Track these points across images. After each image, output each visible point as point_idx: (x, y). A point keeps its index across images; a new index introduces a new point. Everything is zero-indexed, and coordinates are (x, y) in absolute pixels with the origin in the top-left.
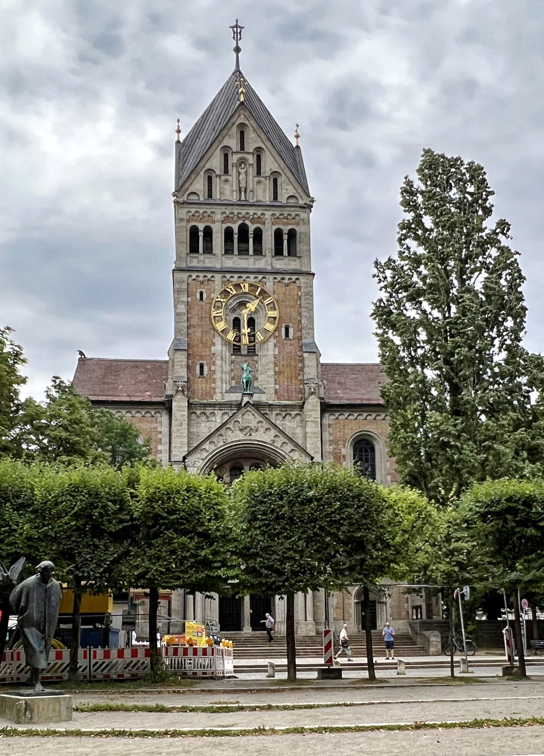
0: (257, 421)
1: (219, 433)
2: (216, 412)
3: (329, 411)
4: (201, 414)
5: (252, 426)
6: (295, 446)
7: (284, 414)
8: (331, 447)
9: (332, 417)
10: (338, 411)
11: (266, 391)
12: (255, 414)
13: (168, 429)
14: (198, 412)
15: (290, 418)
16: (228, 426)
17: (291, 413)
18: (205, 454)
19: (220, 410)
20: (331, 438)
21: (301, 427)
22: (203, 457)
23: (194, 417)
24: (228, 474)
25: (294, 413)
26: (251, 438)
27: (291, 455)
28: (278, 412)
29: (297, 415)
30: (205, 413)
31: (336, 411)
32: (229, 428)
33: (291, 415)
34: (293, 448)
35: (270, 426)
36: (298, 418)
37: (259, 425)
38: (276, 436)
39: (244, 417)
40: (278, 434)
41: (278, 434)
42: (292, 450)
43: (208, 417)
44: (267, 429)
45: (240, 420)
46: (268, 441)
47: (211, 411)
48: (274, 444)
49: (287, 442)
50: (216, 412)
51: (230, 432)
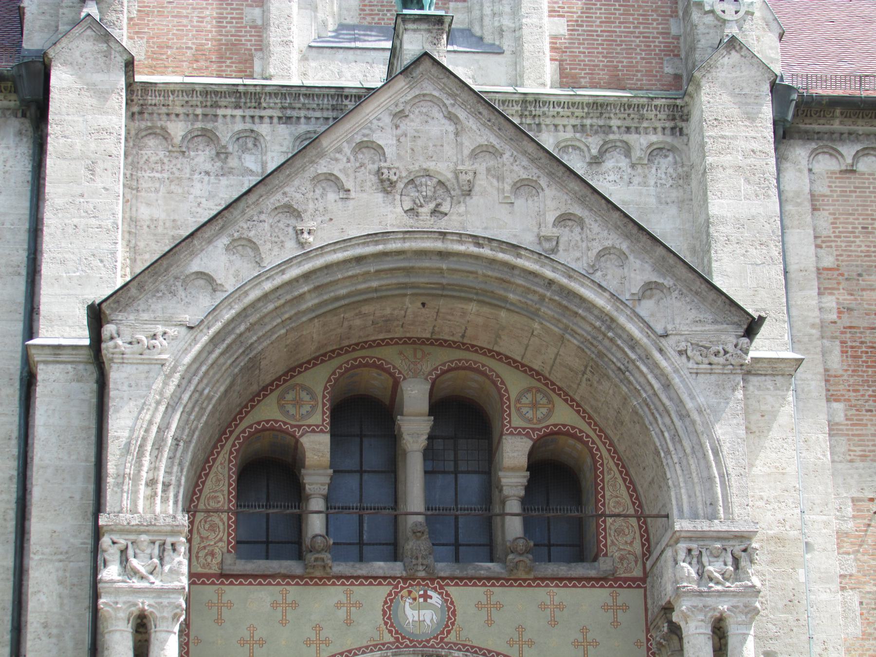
0: (468, 145)
1: (277, 199)
2: (264, 129)
3: (807, 136)
4: (190, 138)
5: (443, 168)
6: (660, 266)
7: (594, 143)
8: (830, 302)
9: (825, 164)
10: (852, 137)
11: (507, 44)
12: (462, 114)
13: (24, 205)
14: (178, 129)
15: (624, 163)
16: (323, 167)
17: (632, 138)
18: (204, 302)
19: (287, 120)
20: (828, 261)
21: (680, 203)
22: (190, 316)
23: (153, 150)
24: (320, 417)
25: (640, 142)
26: (442, 225)
27: (646, 308)
28: (569, 134)
29: (656, 152)
30: (209, 136)
31: (842, 137)
32: (332, 179)
33: (627, 150)
34: (654, 278)
35: (533, 173)
36: (665, 163)
37: (481, 166)
38: (564, 219)
39: (409, 126)
40: (577, 210)
41: (577, 210)
42: (649, 288)
43: (222, 154)
44: (520, 186)
45: (385, 139)
46: (528, 240)
47: (239, 126)
48: (561, 257)
49: (624, 246)
50: (264, 129)
51: (332, 196)
